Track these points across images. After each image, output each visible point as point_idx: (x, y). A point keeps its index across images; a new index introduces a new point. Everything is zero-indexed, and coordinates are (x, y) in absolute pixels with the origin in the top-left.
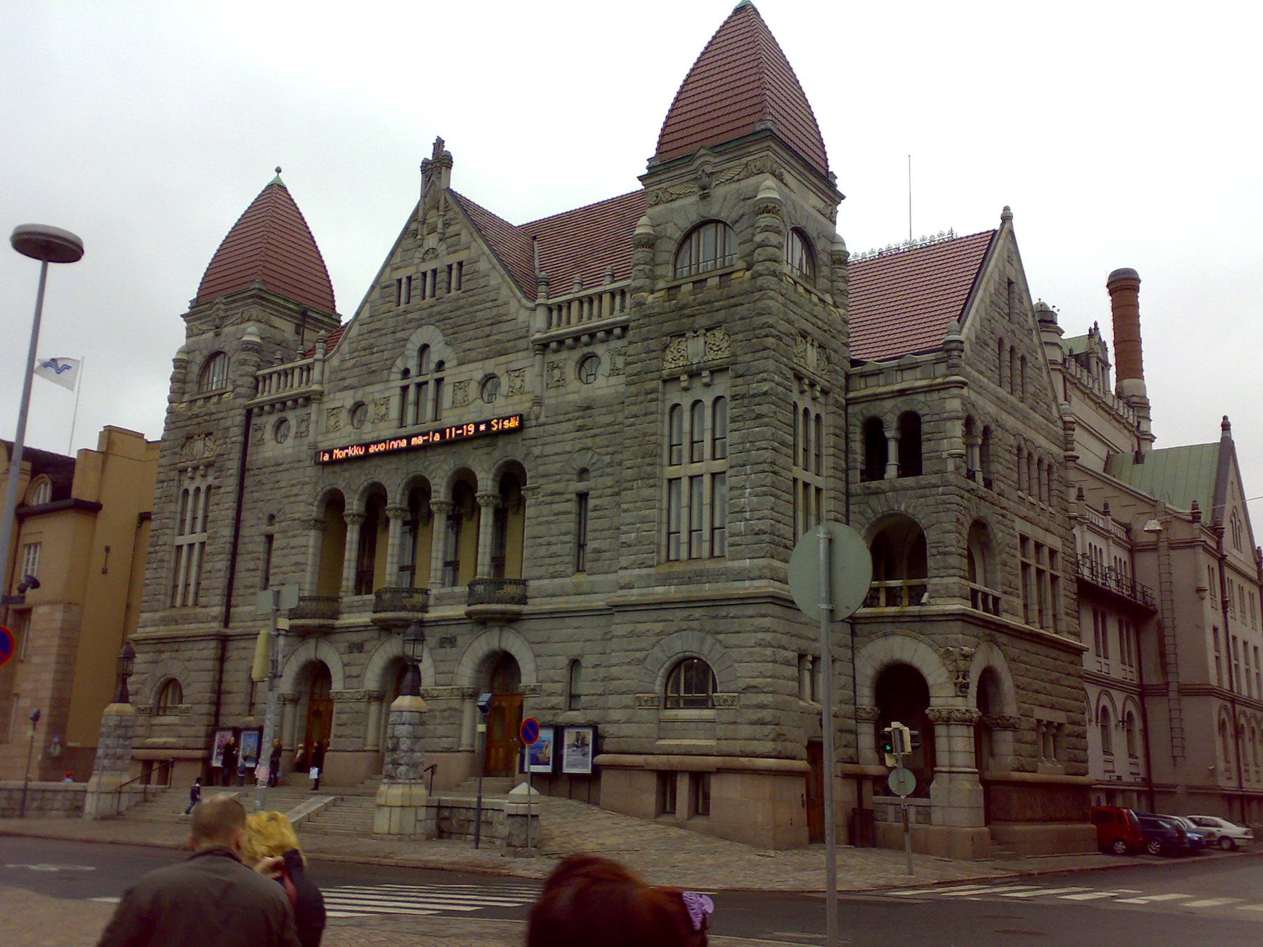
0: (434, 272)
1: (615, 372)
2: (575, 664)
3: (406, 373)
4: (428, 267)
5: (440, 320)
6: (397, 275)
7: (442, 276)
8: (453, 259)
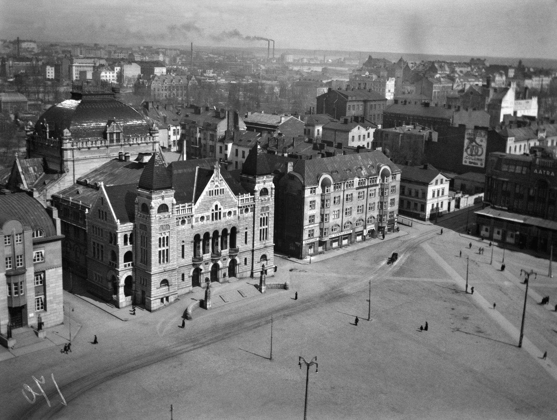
0: (218, 190)
1: (251, 211)
2: (246, 259)
3: (213, 210)
4: (216, 189)
5: (220, 200)
6: (210, 190)
7: (219, 191)
8: (222, 188)
